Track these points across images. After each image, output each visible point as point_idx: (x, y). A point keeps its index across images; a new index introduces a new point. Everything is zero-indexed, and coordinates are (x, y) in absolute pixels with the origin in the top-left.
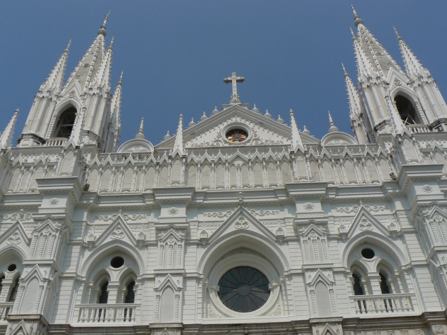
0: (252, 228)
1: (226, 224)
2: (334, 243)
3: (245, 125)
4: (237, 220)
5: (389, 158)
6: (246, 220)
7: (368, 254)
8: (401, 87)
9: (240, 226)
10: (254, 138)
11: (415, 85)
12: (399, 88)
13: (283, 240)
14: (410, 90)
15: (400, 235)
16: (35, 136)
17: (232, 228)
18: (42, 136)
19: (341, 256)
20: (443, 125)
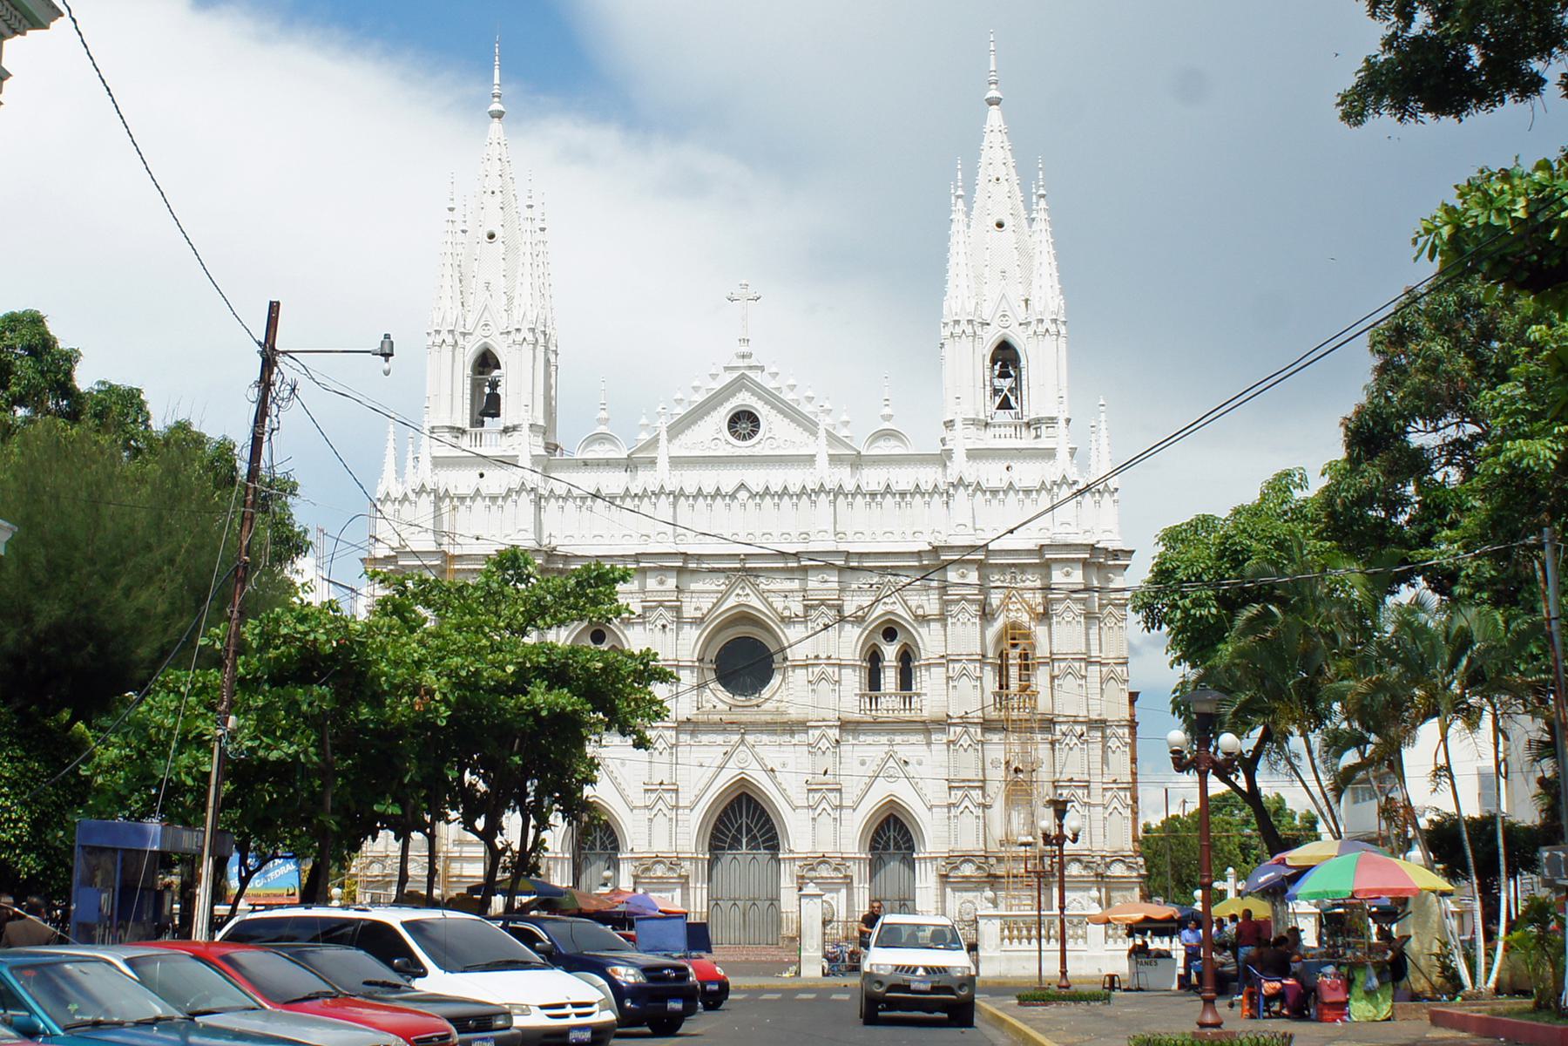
0: (754, 602)
1: (724, 596)
2: (848, 627)
3: (756, 410)
4: (738, 591)
5: (945, 495)
6: (748, 591)
7: (890, 634)
8: (1005, 330)
9: (741, 599)
10: (768, 435)
11: (1030, 331)
12: (1004, 334)
13: (787, 621)
14: (1020, 340)
15: (924, 619)
16: (452, 428)
17: (731, 602)
18: (460, 426)
19: (854, 643)
20: (1044, 427)
